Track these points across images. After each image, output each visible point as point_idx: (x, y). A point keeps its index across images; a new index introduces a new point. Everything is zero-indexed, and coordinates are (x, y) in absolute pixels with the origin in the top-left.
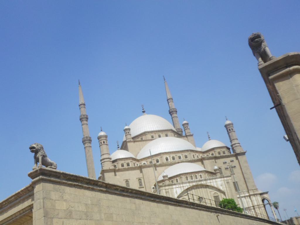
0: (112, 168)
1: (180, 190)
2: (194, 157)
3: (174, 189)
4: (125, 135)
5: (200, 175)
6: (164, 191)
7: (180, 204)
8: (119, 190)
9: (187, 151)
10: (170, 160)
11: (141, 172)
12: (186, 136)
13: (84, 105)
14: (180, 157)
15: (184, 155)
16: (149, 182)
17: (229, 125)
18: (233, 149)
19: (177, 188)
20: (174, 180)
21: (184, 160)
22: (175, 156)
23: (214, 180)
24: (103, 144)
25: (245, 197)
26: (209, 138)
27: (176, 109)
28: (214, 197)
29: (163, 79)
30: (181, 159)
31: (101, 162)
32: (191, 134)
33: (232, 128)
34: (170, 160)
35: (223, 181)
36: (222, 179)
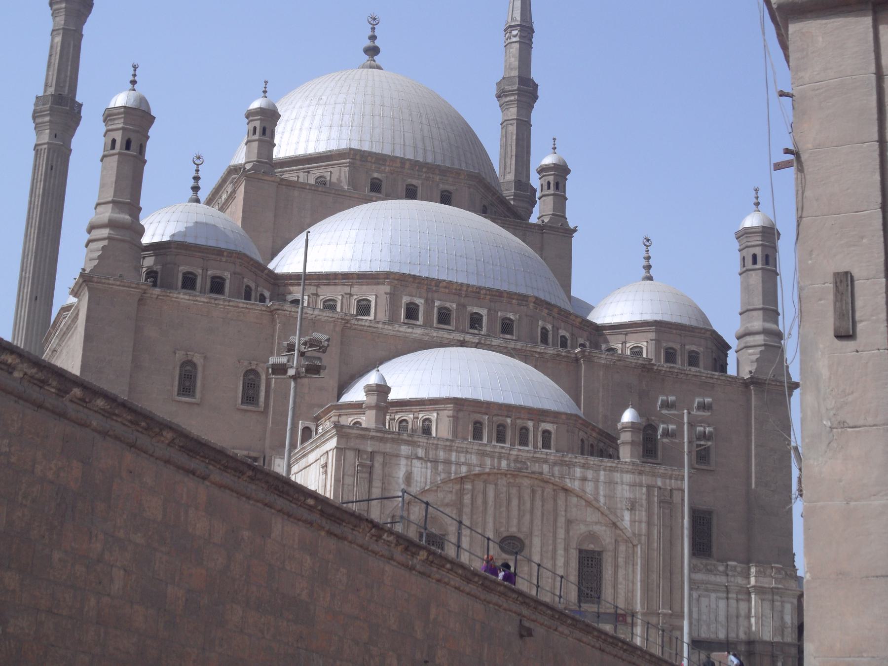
1: (429, 471)
2: (544, 340)
3: (403, 462)
7: (336, 529)
8: (17, 374)
9: (523, 299)
14: (475, 321)
19: (416, 463)
22: (455, 306)
26: (648, 268)
27: (536, 86)
30: (481, 327)
31: (87, 237)
35: (644, 489)
36: (645, 479)
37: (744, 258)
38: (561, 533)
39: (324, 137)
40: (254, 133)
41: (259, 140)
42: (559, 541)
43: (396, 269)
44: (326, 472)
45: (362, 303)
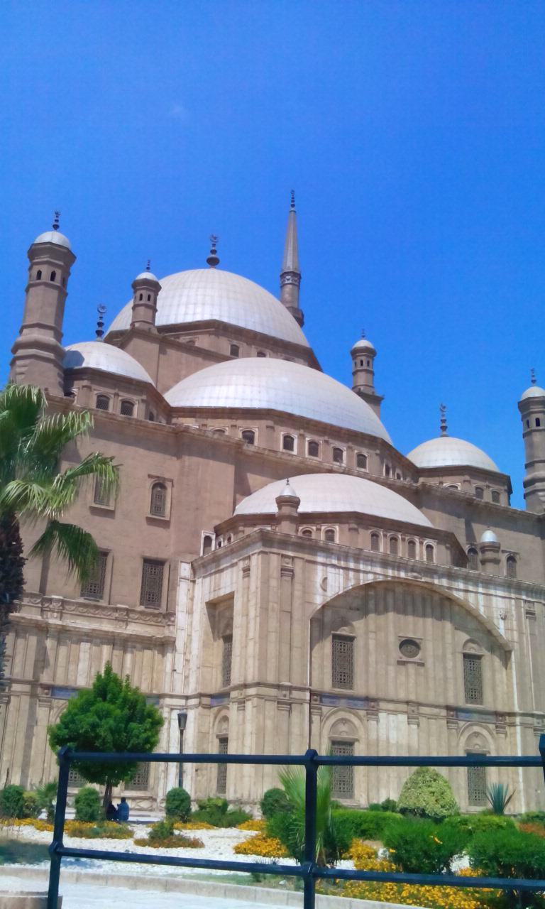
1: (341, 577)
2: (387, 472)
3: (320, 568)
4: (131, 304)
5: (429, 547)
9: (372, 441)
10: (299, 451)
14: (338, 455)
15: (356, 451)
16: (197, 509)
19: (330, 570)
20: (319, 530)
26: (444, 428)
27: (303, 315)
28: (466, 656)
29: (291, 199)
31: (11, 356)
32: (378, 394)
35: (513, 601)
37: (528, 422)
38: (449, 637)
39: (191, 311)
40: (141, 299)
41: (147, 306)
42: (447, 645)
43: (273, 407)
44: (248, 576)
45: (247, 434)
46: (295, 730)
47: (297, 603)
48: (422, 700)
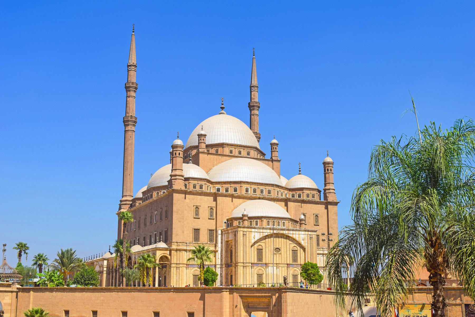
0: (183, 188)
2: (278, 195)
6: (242, 233)
9: (272, 185)
11: (215, 200)
12: (272, 161)
13: (136, 66)
14: (262, 191)
17: (329, 163)
18: (325, 194)
21: (267, 197)
23: (297, 232)
24: (178, 156)
25: (323, 254)
26: (300, 171)
32: (279, 159)
33: (331, 168)
34: (251, 192)
36: (307, 233)
38: (288, 247)
46: (248, 273)
47: (247, 243)
48: (280, 263)
